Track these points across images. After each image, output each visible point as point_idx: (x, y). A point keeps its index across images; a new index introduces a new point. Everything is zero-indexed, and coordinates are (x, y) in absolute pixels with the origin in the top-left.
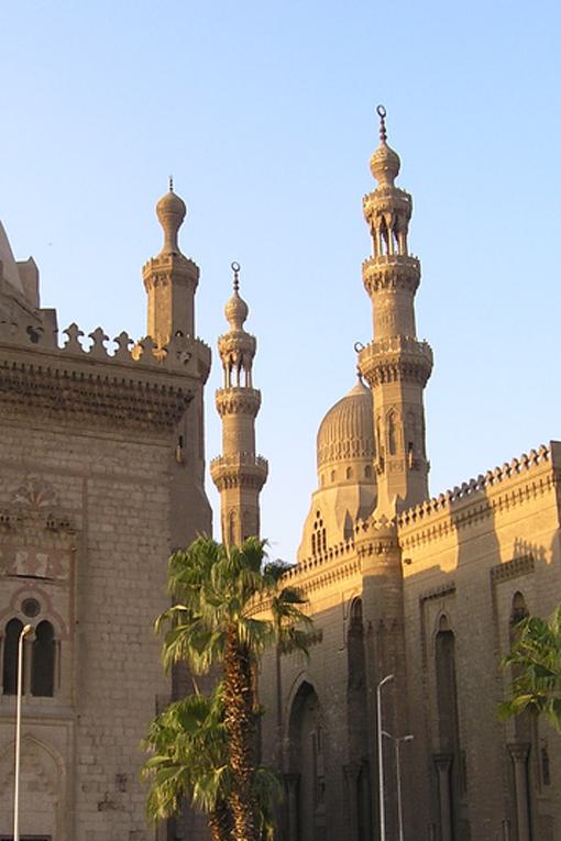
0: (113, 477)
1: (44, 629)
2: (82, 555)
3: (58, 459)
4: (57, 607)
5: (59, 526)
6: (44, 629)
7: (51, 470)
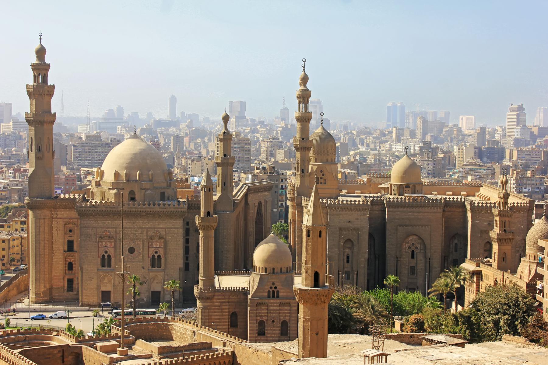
0: (171, 228)
1: (159, 256)
2: (166, 243)
3: (160, 226)
4: (161, 252)
5: (160, 238)
6: (159, 256)
7: (159, 228)
